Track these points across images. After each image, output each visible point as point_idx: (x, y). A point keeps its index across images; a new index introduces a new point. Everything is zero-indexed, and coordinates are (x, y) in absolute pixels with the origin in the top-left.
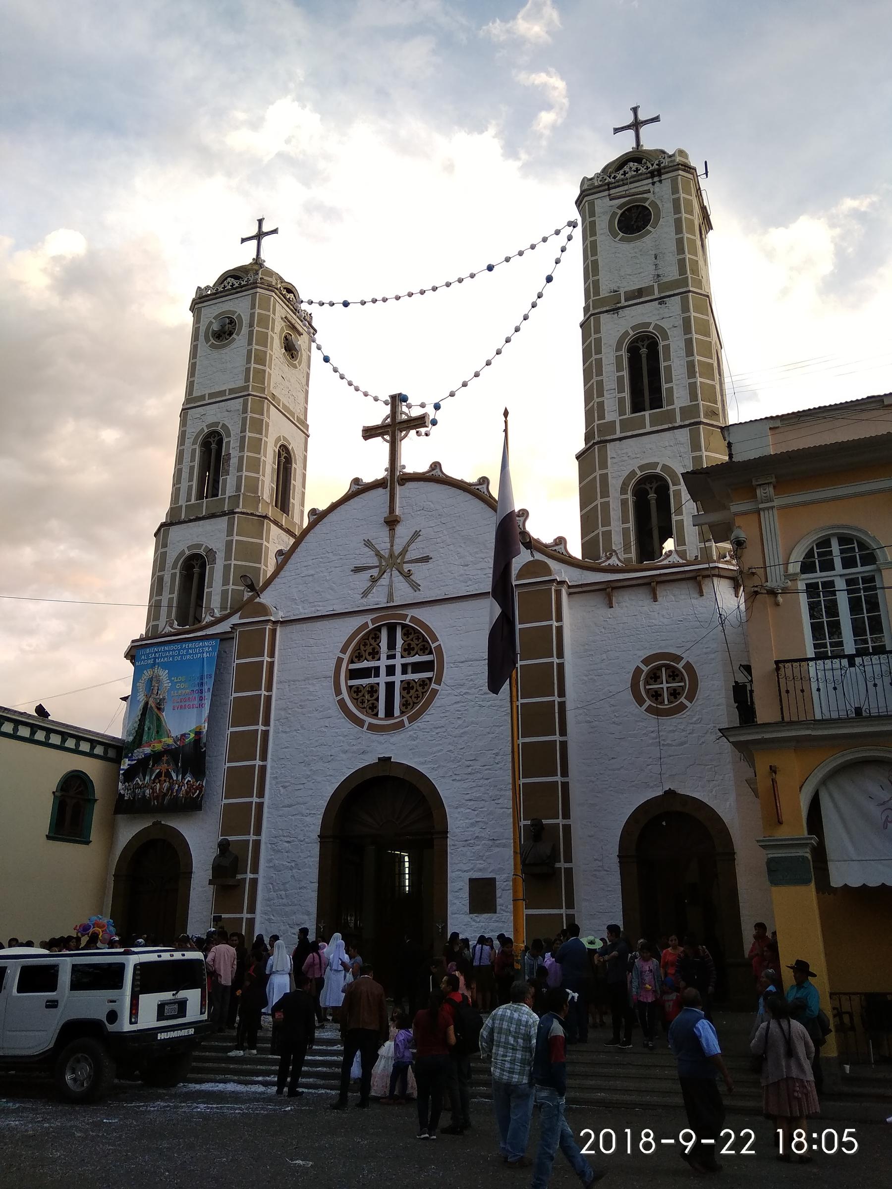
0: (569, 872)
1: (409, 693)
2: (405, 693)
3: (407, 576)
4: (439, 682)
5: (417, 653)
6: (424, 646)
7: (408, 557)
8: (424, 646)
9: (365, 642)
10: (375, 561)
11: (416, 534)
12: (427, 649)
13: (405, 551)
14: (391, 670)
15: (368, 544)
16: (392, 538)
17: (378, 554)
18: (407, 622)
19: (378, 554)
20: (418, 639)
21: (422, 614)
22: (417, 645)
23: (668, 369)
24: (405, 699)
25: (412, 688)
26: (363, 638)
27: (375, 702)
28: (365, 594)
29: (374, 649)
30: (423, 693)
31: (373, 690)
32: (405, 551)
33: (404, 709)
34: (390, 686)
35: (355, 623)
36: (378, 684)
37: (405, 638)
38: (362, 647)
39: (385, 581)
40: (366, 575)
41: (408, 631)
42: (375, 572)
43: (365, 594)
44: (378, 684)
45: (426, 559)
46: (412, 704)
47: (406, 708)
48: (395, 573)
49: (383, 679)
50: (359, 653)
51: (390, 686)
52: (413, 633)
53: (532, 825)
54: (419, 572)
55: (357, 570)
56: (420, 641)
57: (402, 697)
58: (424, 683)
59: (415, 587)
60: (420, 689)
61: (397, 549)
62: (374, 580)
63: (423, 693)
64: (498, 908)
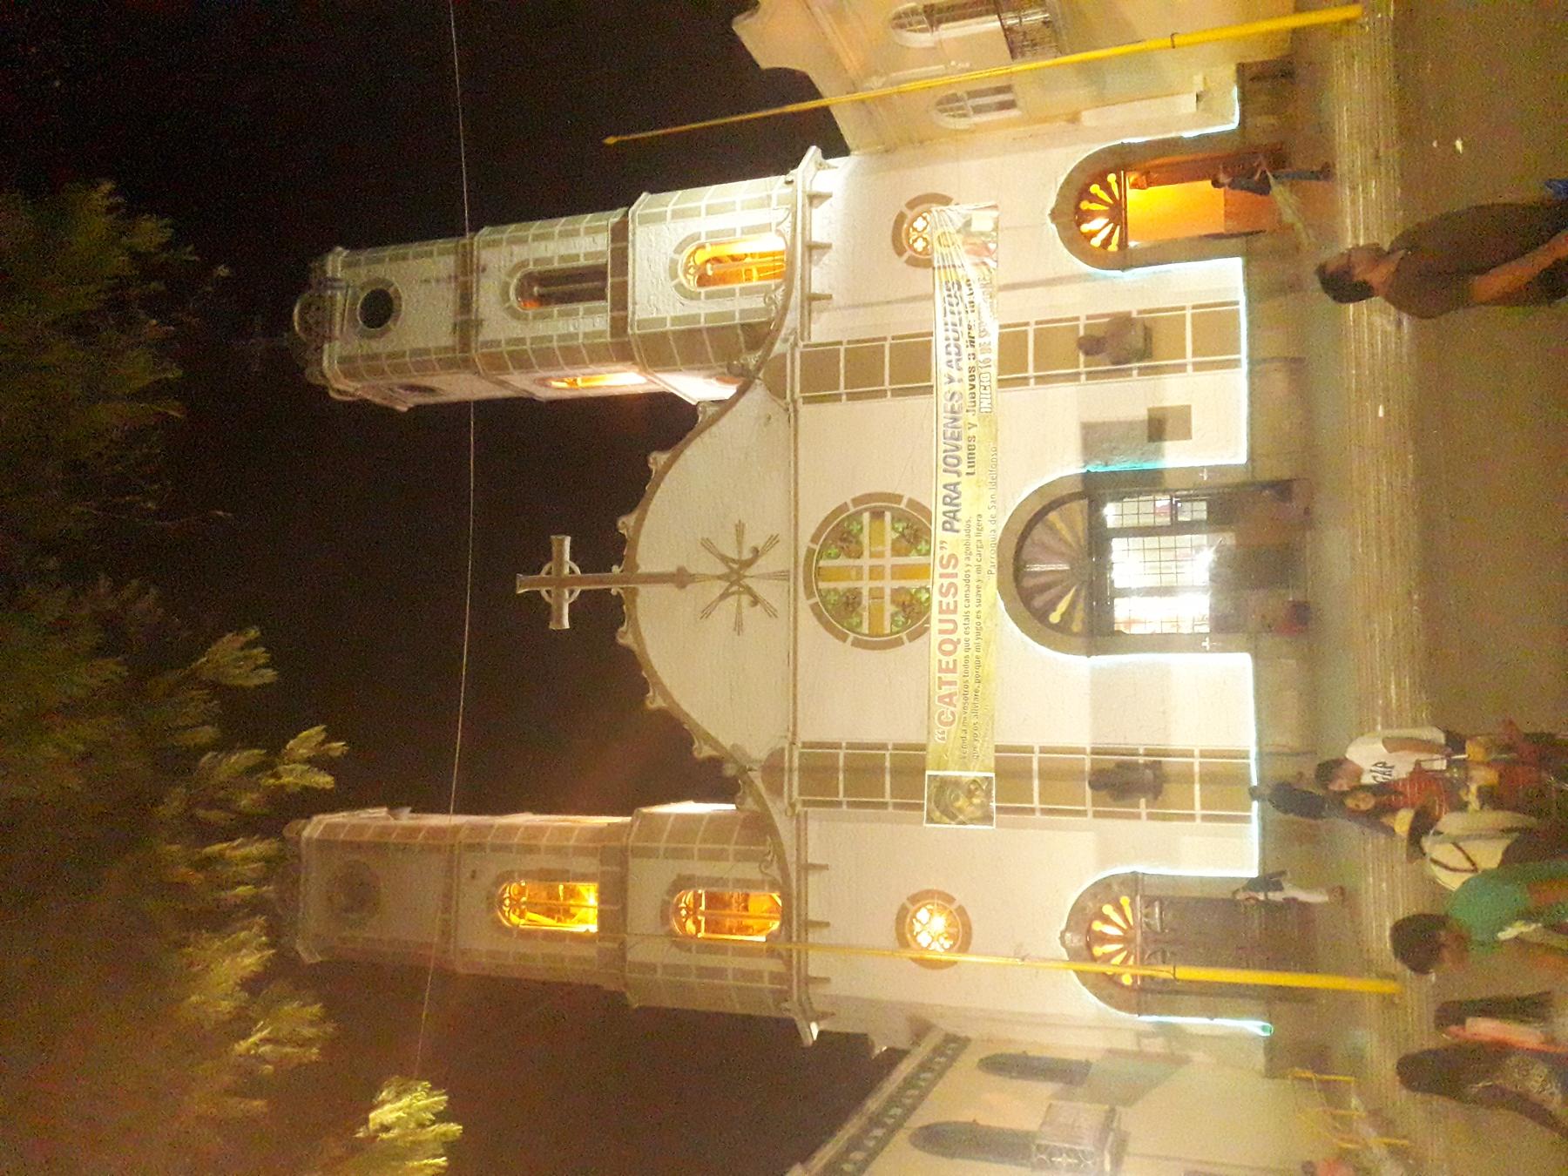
0: (1140, 312)
3: (756, 553)
7: (733, 554)
10: (732, 600)
11: (707, 545)
13: (724, 559)
14: (876, 573)
15: (706, 613)
16: (705, 578)
17: (724, 596)
18: (817, 548)
19: (724, 596)
21: (808, 529)
23: (562, 258)
28: (772, 613)
32: (724, 559)
35: (807, 620)
39: (760, 588)
40: (747, 610)
42: (746, 599)
43: (772, 613)
45: (740, 529)
48: (752, 571)
53: (1087, 353)
54: (754, 538)
55: (739, 627)
59: (773, 540)
61: (722, 569)
62: (755, 601)
64: (1186, 403)
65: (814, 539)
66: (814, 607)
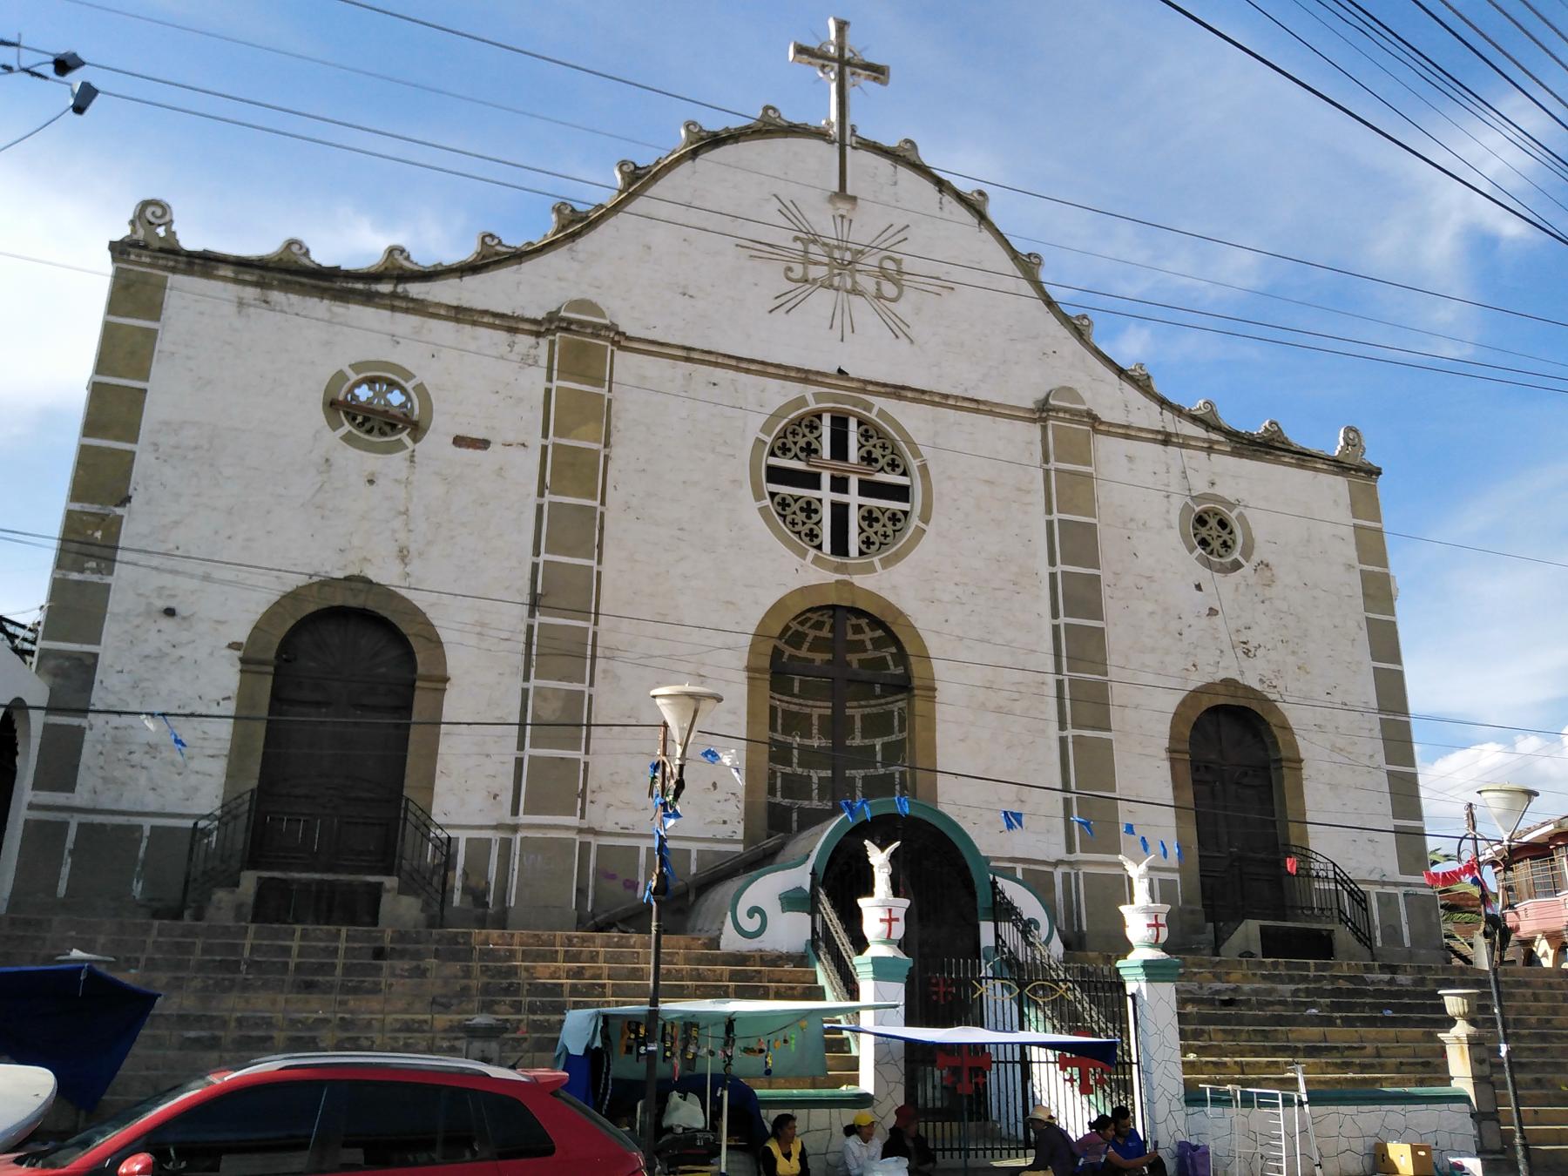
1: (870, 526)
2: (865, 525)
4: (925, 518)
5: (882, 469)
6: (893, 460)
8: (893, 460)
9: (794, 430)
12: (898, 466)
14: (840, 485)
18: (873, 416)
20: (884, 447)
22: (884, 456)
24: (864, 534)
25: (877, 520)
26: (792, 422)
27: (814, 527)
29: (809, 444)
30: (894, 531)
31: (810, 509)
33: (864, 548)
34: (840, 512)
36: (820, 500)
37: (862, 440)
38: (790, 436)
41: (867, 431)
44: (820, 500)
46: (877, 546)
47: (868, 548)
49: (826, 495)
50: (784, 444)
51: (840, 512)
52: (875, 438)
56: (888, 451)
57: (862, 530)
58: (894, 518)
60: (889, 524)
63: (894, 531)
65: (882, 413)
66: (801, 401)
